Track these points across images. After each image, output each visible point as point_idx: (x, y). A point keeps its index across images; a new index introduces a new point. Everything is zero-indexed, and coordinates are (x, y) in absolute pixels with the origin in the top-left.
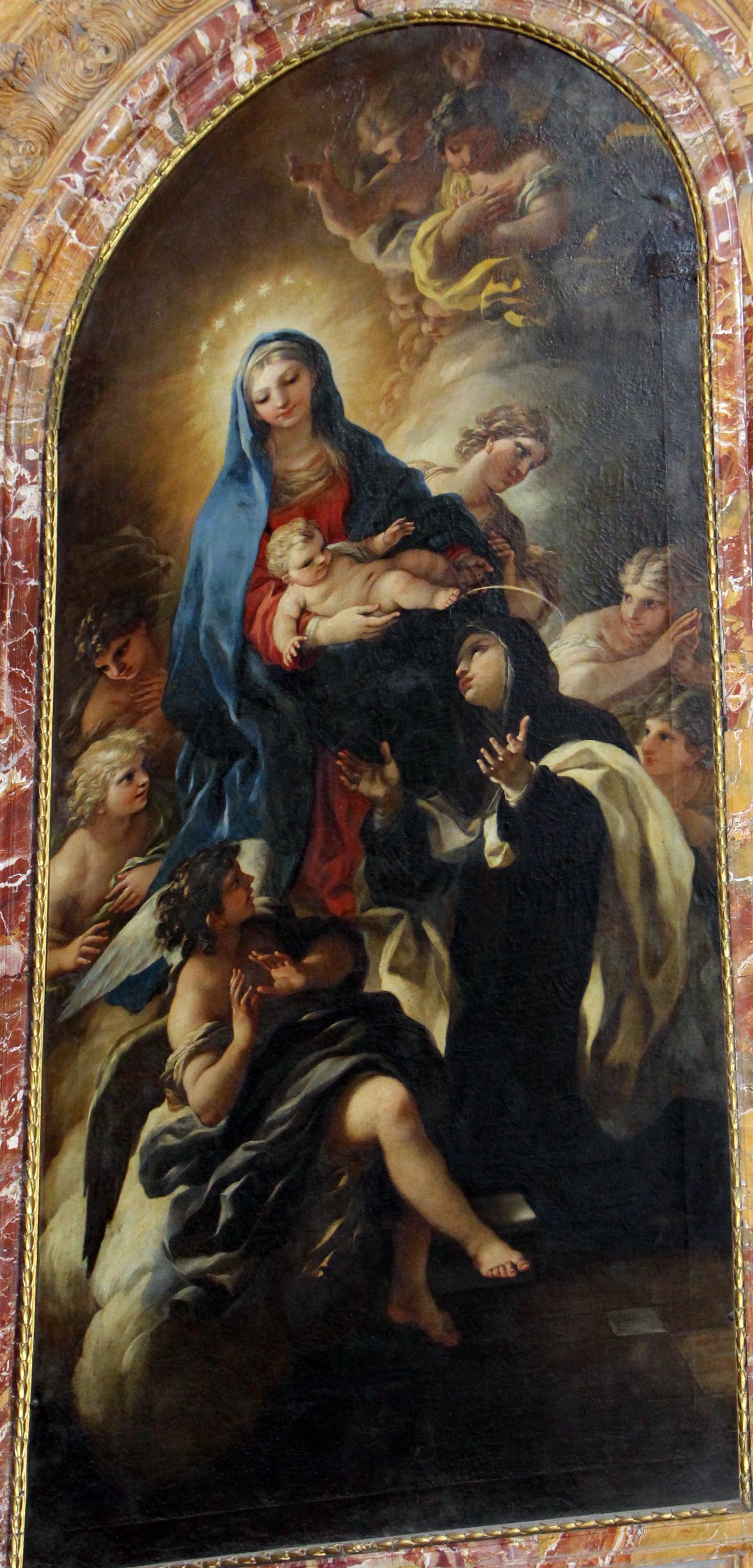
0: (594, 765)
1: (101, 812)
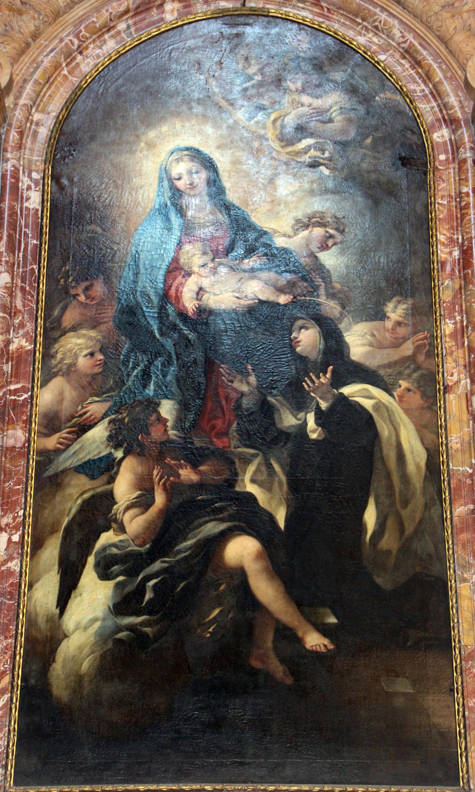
0: (371, 397)
1: (73, 369)
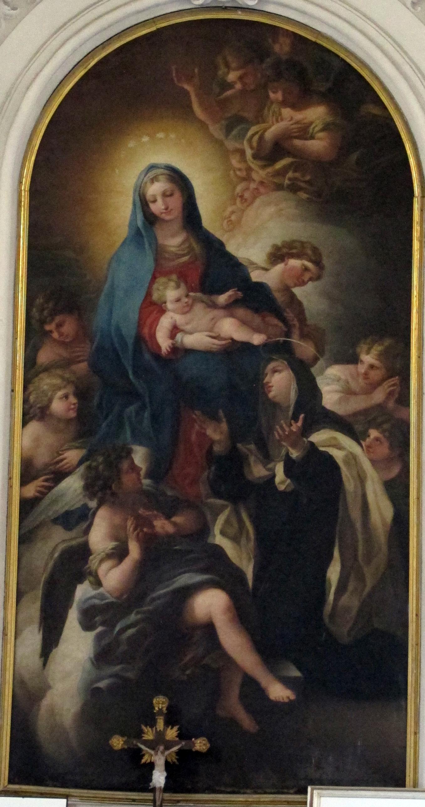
0: (339, 447)
